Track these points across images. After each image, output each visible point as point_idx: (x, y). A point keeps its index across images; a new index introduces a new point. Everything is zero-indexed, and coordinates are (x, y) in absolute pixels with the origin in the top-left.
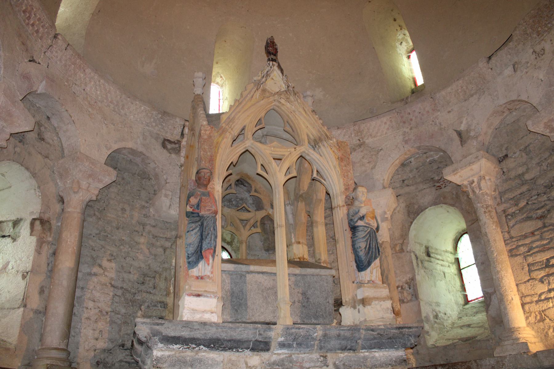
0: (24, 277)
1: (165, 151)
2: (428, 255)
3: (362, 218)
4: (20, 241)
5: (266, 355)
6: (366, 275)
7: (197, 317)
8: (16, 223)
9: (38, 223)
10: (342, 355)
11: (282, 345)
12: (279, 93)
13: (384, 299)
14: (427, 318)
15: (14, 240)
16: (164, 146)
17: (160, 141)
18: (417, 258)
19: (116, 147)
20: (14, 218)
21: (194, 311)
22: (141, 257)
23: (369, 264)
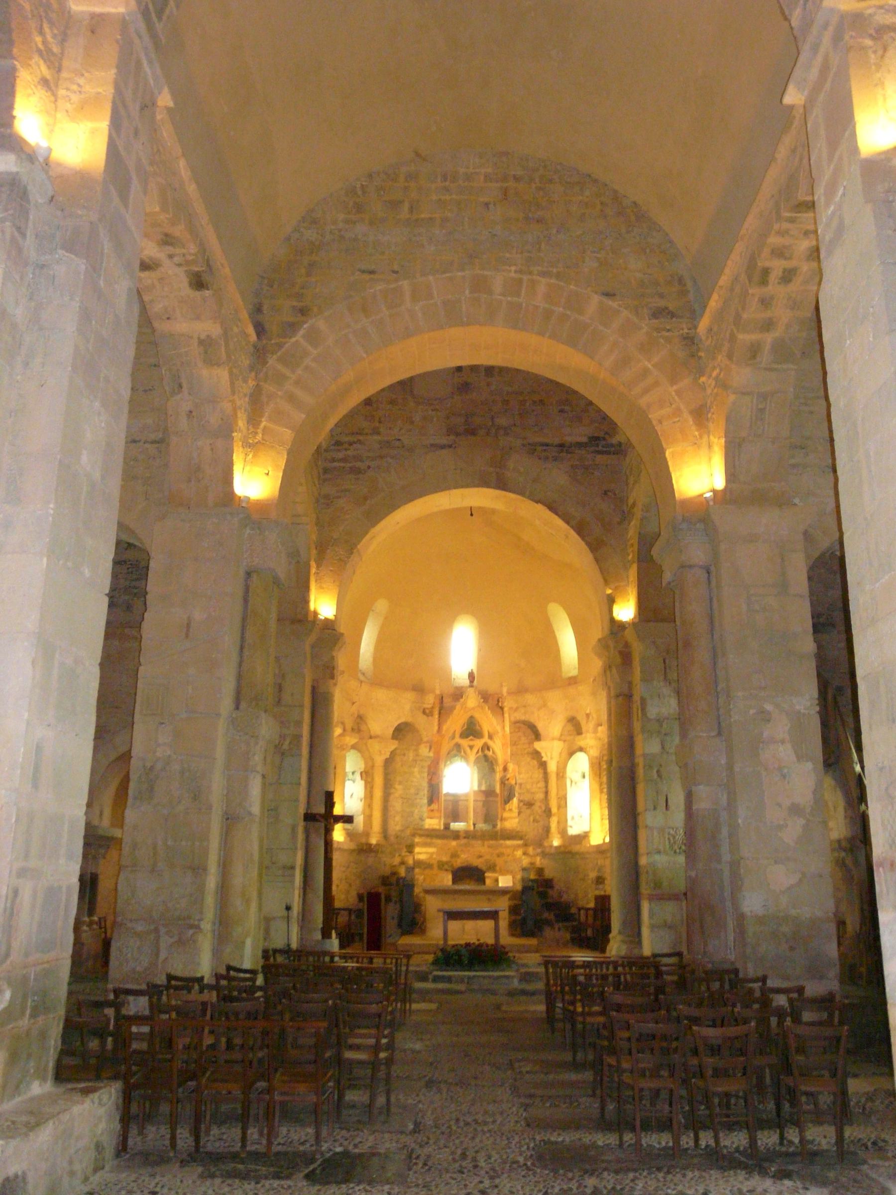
0: (361, 800)
1: (425, 716)
2: (584, 777)
3: (508, 779)
4: (357, 782)
5: (458, 841)
6: (507, 807)
7: (431, 827)
8: (353, 773)
9: (364, 774)
10: (491, 842)
11: (465, 838)
12: (473, 709)
13: (514, 818)
14: (573, 818)
15: (354, 782)
16: (424, 712)
17: (422, 710)
18: (572, 782)
19: (396, 724)
20: (352, 771)
21: (430, 825)
22: (415, 780)
23: (509, 802)
